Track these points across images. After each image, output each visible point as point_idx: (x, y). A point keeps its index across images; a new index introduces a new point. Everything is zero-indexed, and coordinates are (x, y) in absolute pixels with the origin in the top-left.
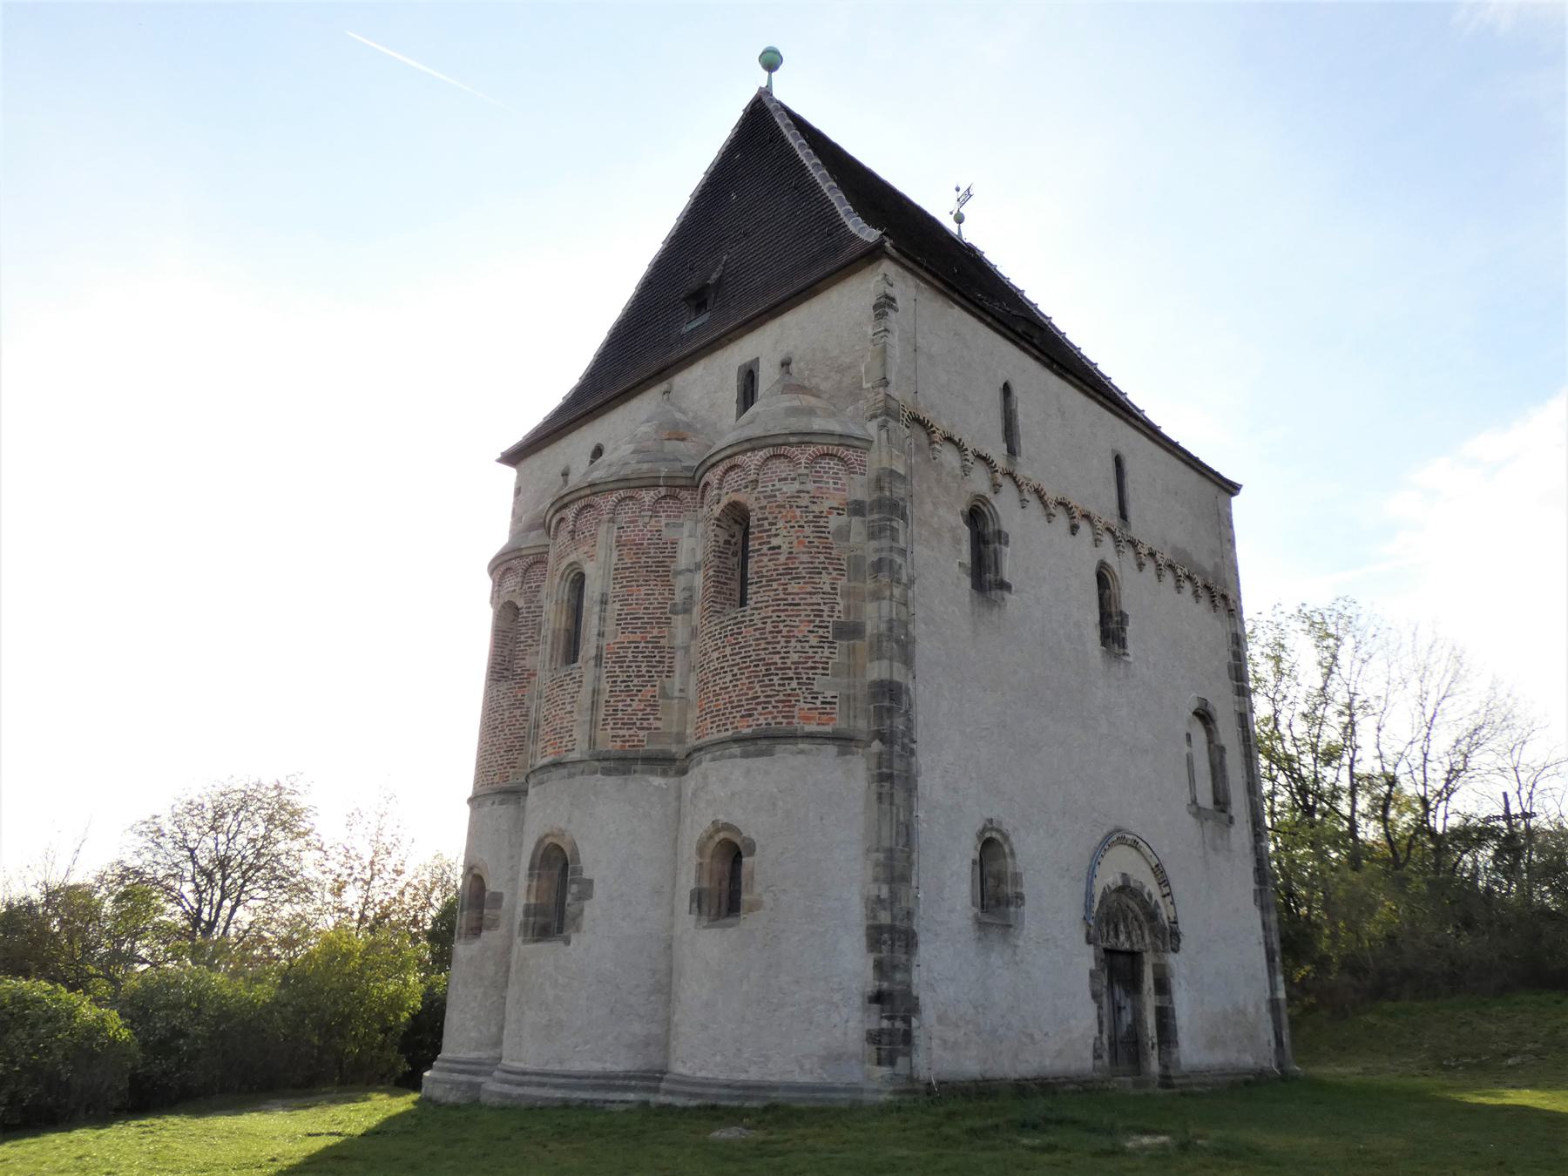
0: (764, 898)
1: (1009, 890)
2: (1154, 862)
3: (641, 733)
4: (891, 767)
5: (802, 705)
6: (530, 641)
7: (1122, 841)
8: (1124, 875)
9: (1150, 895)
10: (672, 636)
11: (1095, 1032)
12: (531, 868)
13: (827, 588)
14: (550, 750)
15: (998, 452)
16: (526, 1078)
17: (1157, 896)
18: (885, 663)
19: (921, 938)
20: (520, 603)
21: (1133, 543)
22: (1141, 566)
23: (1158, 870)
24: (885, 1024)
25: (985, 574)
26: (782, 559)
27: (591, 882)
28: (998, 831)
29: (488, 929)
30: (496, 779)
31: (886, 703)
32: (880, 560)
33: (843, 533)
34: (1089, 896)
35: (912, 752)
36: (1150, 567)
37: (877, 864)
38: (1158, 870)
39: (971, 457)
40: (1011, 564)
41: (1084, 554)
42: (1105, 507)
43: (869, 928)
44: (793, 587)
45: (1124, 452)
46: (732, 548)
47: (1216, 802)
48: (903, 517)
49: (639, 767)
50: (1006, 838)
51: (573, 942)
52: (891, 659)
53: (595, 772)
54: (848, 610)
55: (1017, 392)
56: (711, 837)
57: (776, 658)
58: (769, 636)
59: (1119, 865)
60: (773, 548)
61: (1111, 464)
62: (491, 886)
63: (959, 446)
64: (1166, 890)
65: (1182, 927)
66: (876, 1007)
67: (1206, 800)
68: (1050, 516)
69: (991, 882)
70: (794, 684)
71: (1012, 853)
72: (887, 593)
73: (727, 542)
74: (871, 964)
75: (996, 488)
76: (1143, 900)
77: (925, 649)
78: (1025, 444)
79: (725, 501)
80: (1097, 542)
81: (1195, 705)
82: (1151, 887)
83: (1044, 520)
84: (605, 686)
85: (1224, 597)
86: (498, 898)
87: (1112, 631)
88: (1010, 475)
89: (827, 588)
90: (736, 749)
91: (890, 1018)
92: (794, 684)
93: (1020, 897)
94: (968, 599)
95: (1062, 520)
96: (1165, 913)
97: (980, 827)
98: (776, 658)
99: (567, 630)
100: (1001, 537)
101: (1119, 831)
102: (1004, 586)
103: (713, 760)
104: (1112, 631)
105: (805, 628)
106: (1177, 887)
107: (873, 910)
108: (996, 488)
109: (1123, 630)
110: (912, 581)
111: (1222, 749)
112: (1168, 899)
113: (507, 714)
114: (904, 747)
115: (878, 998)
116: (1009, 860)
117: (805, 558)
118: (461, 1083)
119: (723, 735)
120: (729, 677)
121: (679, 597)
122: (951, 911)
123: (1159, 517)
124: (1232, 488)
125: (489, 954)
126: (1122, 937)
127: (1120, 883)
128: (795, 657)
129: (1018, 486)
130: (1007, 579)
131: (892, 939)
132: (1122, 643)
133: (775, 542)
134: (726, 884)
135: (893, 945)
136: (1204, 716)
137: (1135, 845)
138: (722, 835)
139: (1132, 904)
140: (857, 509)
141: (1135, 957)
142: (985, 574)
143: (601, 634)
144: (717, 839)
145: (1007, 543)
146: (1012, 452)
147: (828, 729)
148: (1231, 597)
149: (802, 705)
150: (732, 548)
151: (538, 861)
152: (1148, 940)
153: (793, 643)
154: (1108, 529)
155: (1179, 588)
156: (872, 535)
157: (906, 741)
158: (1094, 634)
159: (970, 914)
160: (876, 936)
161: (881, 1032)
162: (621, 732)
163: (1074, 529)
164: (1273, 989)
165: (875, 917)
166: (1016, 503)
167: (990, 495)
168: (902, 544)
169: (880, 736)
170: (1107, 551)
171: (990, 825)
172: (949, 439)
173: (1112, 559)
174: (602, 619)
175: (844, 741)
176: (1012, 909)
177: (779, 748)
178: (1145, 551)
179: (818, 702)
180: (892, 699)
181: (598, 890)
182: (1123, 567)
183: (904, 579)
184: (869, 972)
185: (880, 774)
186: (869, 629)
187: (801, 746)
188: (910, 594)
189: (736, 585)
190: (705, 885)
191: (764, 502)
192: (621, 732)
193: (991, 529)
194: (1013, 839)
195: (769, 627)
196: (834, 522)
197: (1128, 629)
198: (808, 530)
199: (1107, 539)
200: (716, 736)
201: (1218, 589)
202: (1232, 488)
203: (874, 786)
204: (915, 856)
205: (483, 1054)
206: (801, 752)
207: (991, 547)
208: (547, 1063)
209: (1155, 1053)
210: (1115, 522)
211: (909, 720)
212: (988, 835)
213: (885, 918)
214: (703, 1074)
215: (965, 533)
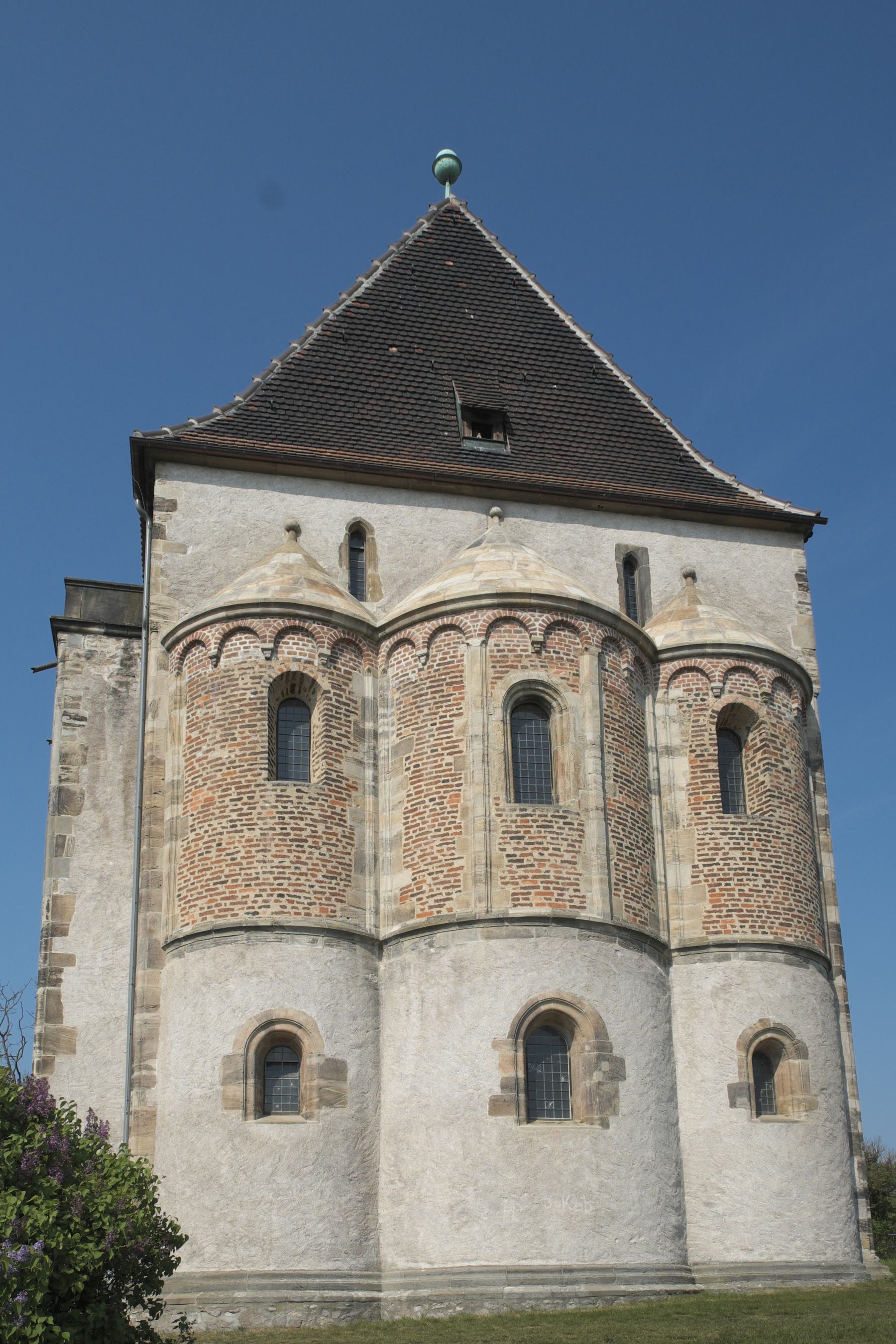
3: (646, 911)
6: (344, 741)
16: (576, 1275)
27: (622, 1061)
30: (315, 910)
51: (613, 1125)
56: (757, 1036)
79: (727, 699)
90: (780, 955)
103: (748, 959)
113: (321, 828)
118: (335, 1301)
119: (760, 937)
120: (760, 882)
125: (338, 1137)
138: (769, 1035)
144: (762, 1038)
162: (634, 904)
200: (749, 936)
205: (343, 1265)
208: (598, 1257)
214: (784, 1258)
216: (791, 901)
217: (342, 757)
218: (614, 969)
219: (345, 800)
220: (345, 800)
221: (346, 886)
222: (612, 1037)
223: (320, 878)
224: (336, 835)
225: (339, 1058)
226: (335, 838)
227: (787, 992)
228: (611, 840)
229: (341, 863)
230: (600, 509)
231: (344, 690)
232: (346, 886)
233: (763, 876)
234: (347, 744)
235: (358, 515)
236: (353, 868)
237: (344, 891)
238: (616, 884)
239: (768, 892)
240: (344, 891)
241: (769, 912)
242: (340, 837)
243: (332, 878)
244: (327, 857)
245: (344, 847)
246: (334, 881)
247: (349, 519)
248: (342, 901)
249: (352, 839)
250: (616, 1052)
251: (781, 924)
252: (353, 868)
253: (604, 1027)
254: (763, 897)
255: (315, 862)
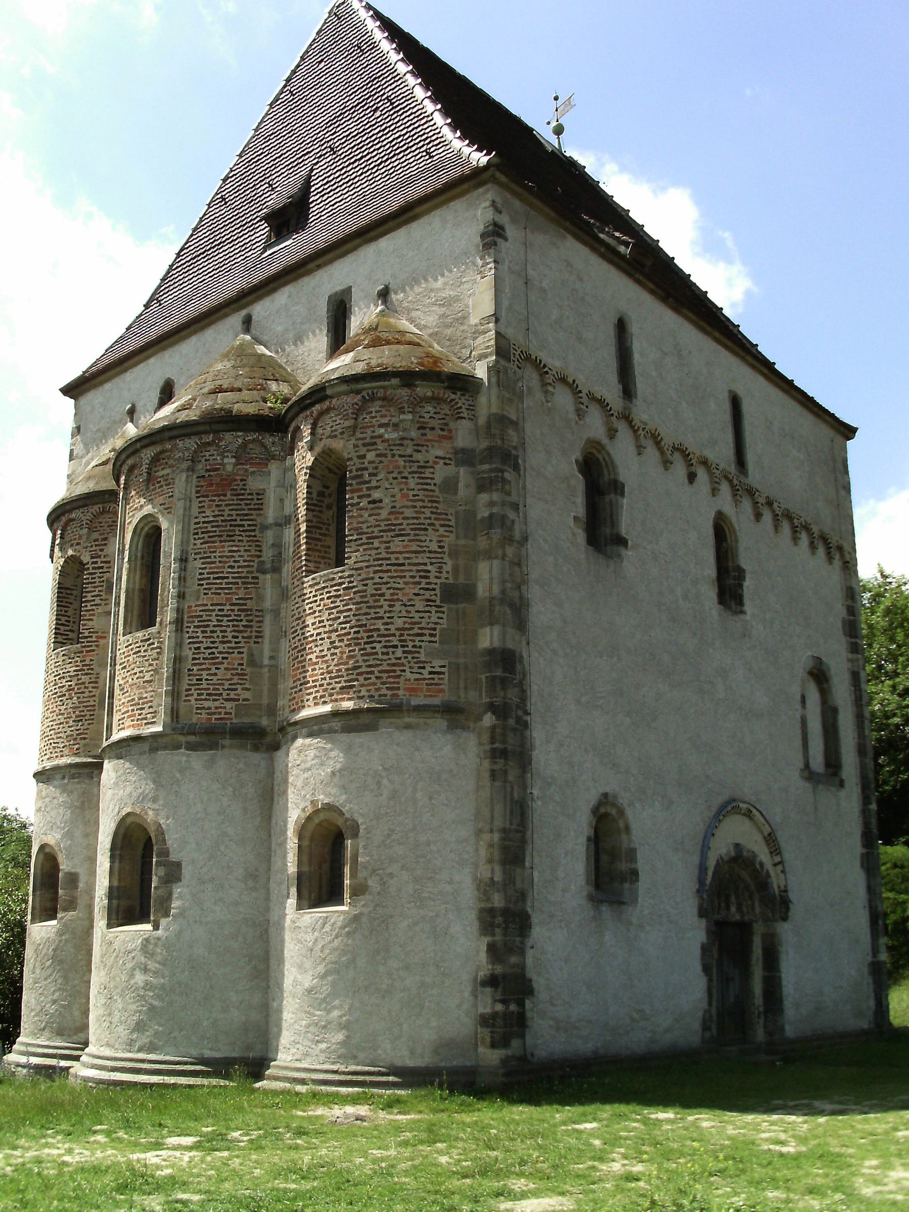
0: (370, 883)
1: (623, 866)
2: (767, 830)
3: (229, 705)
4: (504, 742)
5: (408, 674)
6: (98, 601)
7: (736, 810)
8: (737, 846)
9: (761, 864)
10: (261, 598)
11: (705, 1005)
12: (113, 849)
13: (434, 546)
14: (128, 723)
15: (611, 392)
17: (768, 865)
18: (497, 630)
19: (535, 920)
20: (86, 558)
21: (751, 492)
22: (758, 516)
23: (771, 841)
24: (499, 1007)
25: (601, 532)
26: (384, 514)
27: (179, 865)
28: (614, 805)
29: (65, 910)
31: (499, 673)
32: (491, 516)
33: (450, 486)
34: (703, 868)
35: (526, 725)
36: (767, 517)
37: (491, 846)
38: (771, 841)
39: (585, 400)
40: (630, 516)
41: (701, 505)
42: (722, 453)
43: (482, 911)
44: (397, 544)
45: (741, 392)
46: (327, 501)
47: (828, 765)
48: (516, 468)
49: (227, 742)
50: (621, 812)
52: (504, 625)
53: (178, 747)
54: (456, 570)
55: (634, 328)
57: (379, 624)
58: (371, 600)
59: (736, 833)
60: (374, 502)
61: (727, 406)
62: (65, 866)
63: (575, 391)
64: (777, 859)
65: (792, 896)
66: (488, 990)
67: (818, 762)
68: (666, 463)
69: (604, 858)
70: (399, 652)
71: (627, 829)
72: (500, 552)
73: (321, 494)
74: (484, 948)
75: (612, 433)
76: (755, 870)
77: (541, 613)
78: (641, 386)
80: (714, 492)
81: (810, 664)
82: (764, 856)
83: (661, 469)
84: (188, 653)
85: (840, 549)
86: (73, 879)
87: (729, 589)
88: (627, 418)
89: (434, 546)
90: (336, 724)
91: (503, 1001)
92: (399, 652)
93: (635, 873)
94: (583, 556)
95: (679, 469)
96: (776, 881)
97: (593, 802)
98: (379, 624)
99: (142, 590)
100: (618, 488)
101: (734, 800)
102: (622, 542)
104: (729, 589)
105: (411, 590)
106: (788, 855)
107: (485, 893)
108: (612, 433)
109: (741, 586)
110: (525, 539)
111: (835, 711)
112: (780, 868)
114: (519, 720)
115: (492, 981)
116: (624, 836)
117: (409, 513)
121: (268, 554)
122: (564, 890)
123: (777, 465)
124: (849, 432)
126: (733, 909)
127: (733, 854)
128: (399, 623)
129: (635, 432)
130: (623, 532)
131: (508, 921)
132: (739, 600)
133: (376, 495)
134: (326, 867)
135: (506, 928)
136: (819, 675)
137: (748, 814)
139: (745, 875)
140: (465, 457)
141: (744, 928)
142: (601, 532)
143: (181, 596)
145: (622, 494)
146: (628, 392)
147: (436, 701)
148: (847, 547)
149: (408, 674)
150: (327, 501)
151: (119, 842)
152: (758, 910)
153: (398, 606)
154: (726, 477)
155: (795, 539)
156: (482, 487)
157: (520, 713)
158: (710, 594)
159: (585, 893)
160: (489, 920)
161: (495, 1015)
162: (206, 704)
163: (692, 477)
164: (875, 951)
165: (488, 900)
166: (632, 449)
167: (605, 441)
168: (514, 498)
169: (492, 707)
170: (725, 501)
171: (605, 799)
172: (563, 380)
173: (728, 509)
174: (182, 579)
175: (453, 714)
176: (627, 885)
177: (382, 722)
178: (762, 500)
179: (425, 672)
180: (505, 670)
181: (187, 872)
182: (741, 518)
183: (517, 535)
184: (483, 956)
185: (493, 751)
186: (482, 590)
187: (407, 720)
188: (523, 552)
189: (331, 542)
190: (306, 869)
191: (363, 451)
192: (206, 704)
193: (606, 478)
194: (629, 813)
195: (370, 590)
196: (441, 473)
197: (746, 584)
198: (412, 483)
199: (725, 488)
201: (834, 540)
202: (849, 432)
203: (486, 764)
204: (529, 833)
206: (408, 727)
207: (607, 498)
209: (762, 1021)
210: (732, 468)
211: (523, 691)
212: (602, 810)
213: (498, 901)
215: (579, 482)
216: (360, 659)
217: (94, 615)
218: (178, 775)
219: (93, 651)
220: (93, 651)
221: (89, 724)
222: (169, 843)
223: (71, 723)
224: (84, 683)
225: (73, 870)
226: (83, 686)
227: (338, 766)
228: (186, 647)
229: (86, 707)
230: (319, 267)
231: (99, 557)
232: (89, 724)
233: (329, 638)
234: (99, 602)
235: (168, 376)
236: (97, 708)
237: (88, 729)
238: (187, 690)
239: (332, 654)
240: (88, 729)
241: (331, 678)
242: (87, 685)
243: (79, 721)
244: (77, 705)
245: (90, 692)
246: (80, 723)
247: (161, 383)
248: (85, 739)
249: (96, 682)
250: (173, 857)
251: (342, 688)
252: (97, 708)
253: (163, 834)
254: (326, 662)
255: (70, 710)
